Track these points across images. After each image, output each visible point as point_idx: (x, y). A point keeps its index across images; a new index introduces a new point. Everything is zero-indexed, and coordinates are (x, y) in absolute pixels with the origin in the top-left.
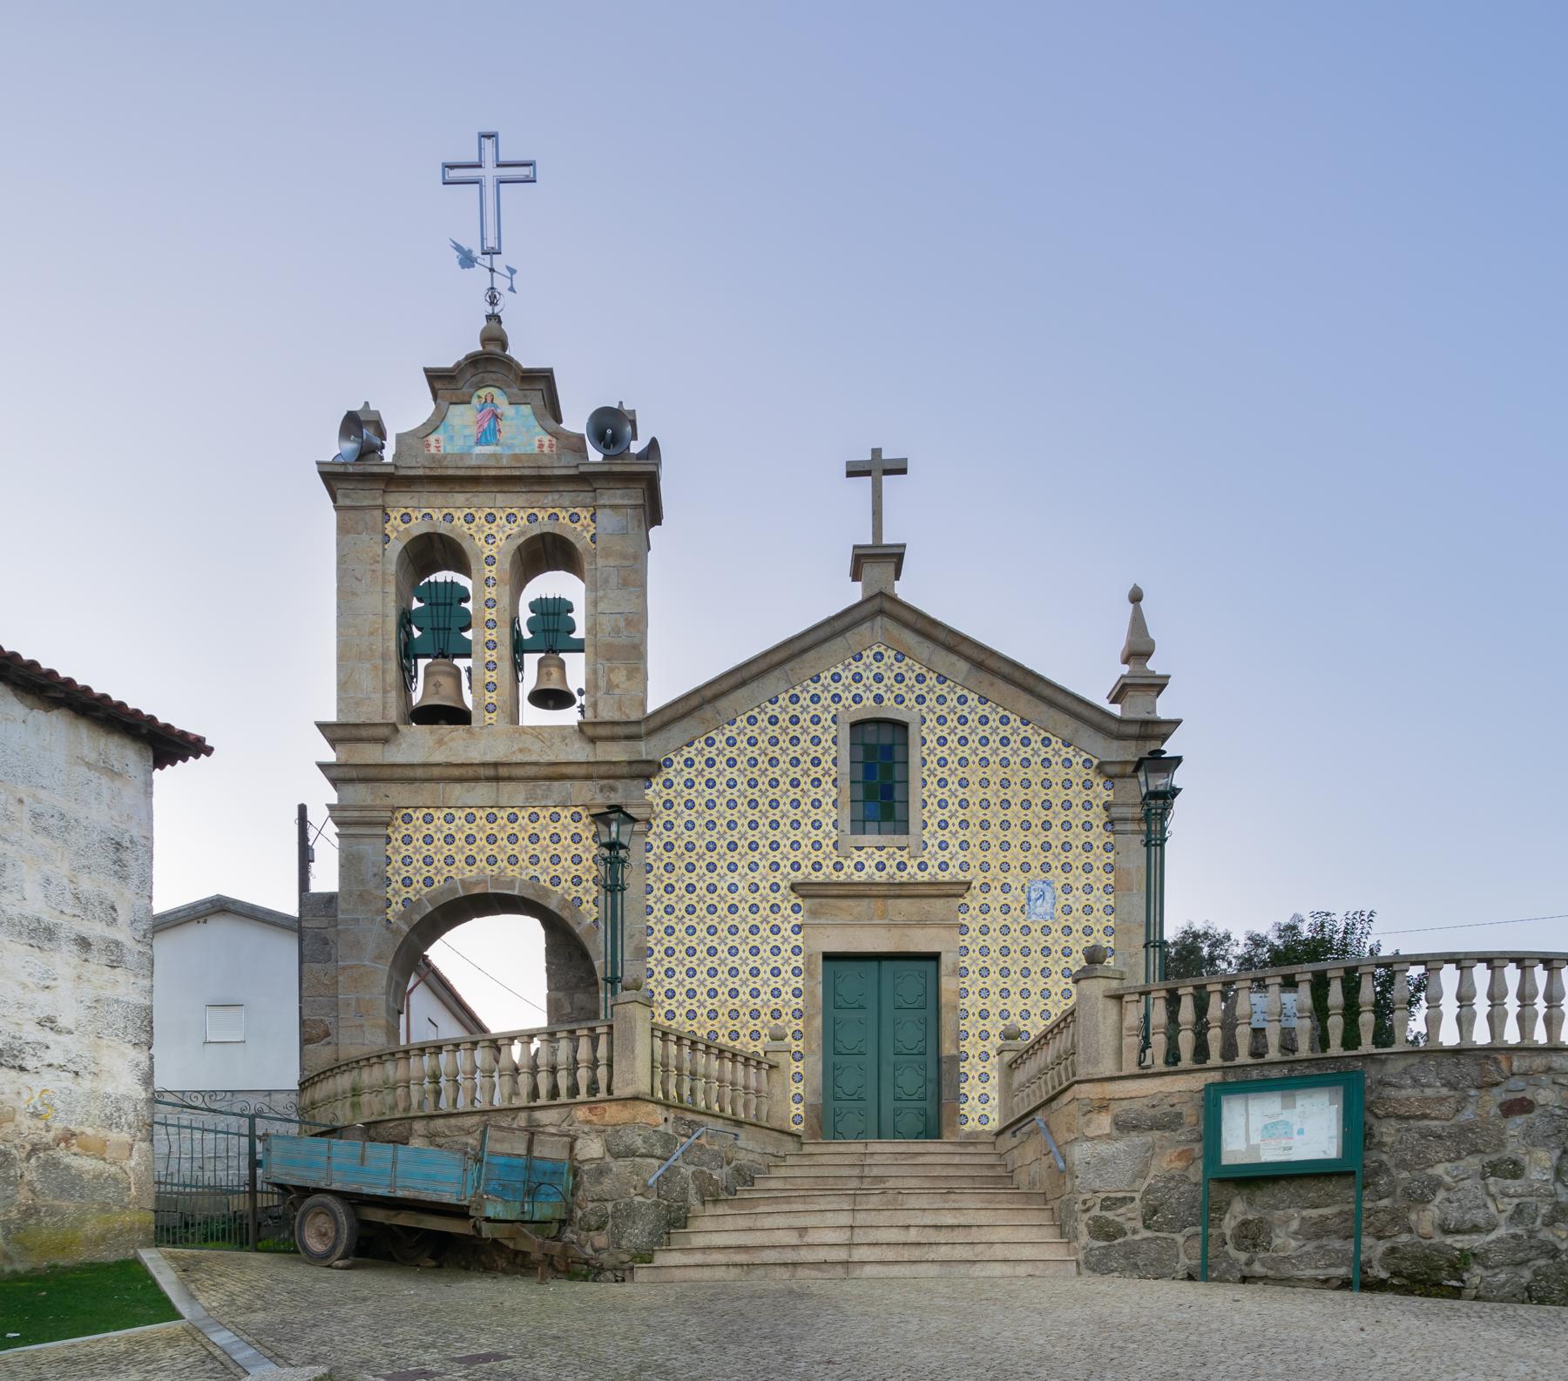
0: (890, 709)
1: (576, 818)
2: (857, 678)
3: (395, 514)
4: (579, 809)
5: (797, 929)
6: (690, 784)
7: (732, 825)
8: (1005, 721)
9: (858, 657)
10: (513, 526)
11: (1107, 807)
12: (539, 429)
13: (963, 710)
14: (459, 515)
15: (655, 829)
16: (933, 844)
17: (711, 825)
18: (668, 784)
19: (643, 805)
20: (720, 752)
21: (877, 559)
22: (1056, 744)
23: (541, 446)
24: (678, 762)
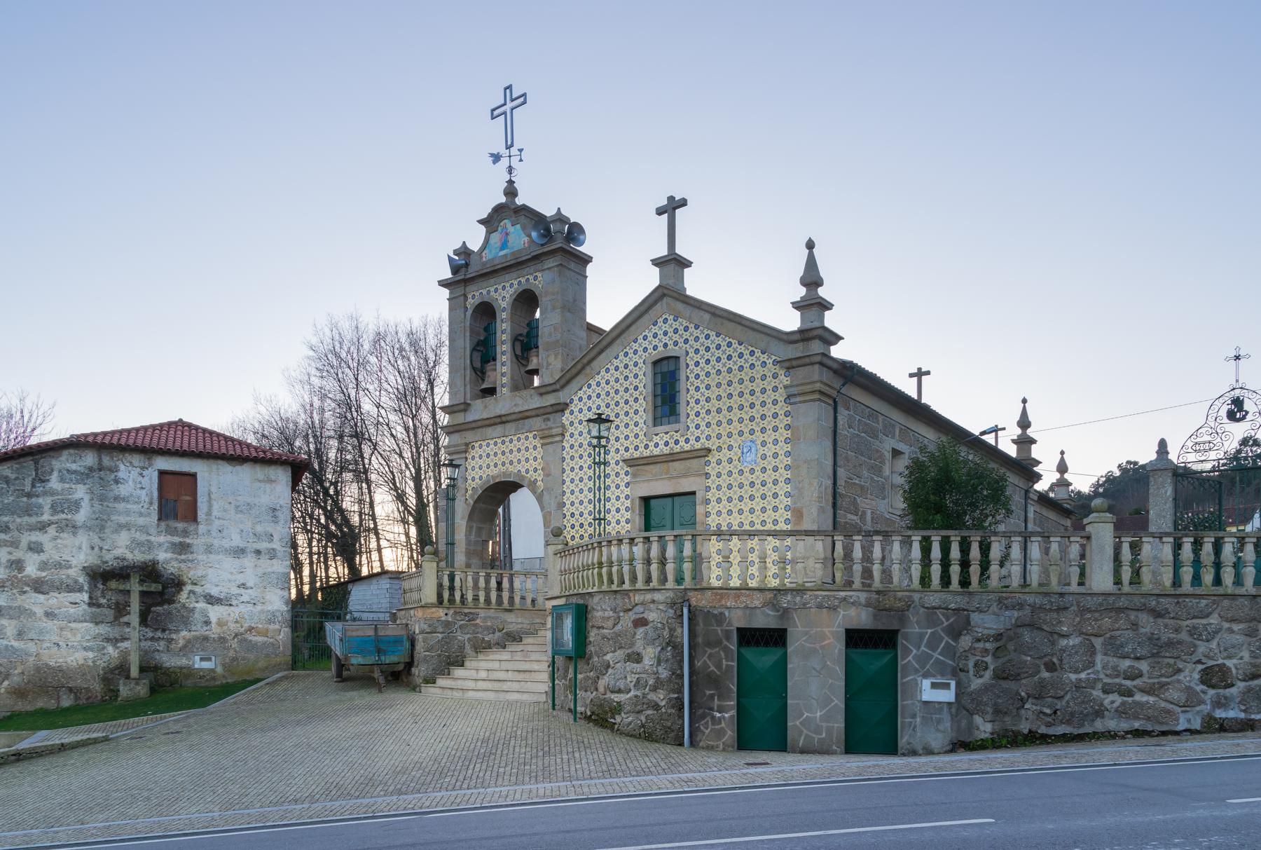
0: (672, 351)
2: (655, 336)
5: (627, 485)
8: (729, 345)
9: (655, 324)
11: (786, 387)
13: (708, 343)
16: (692, 426)
21: (673, 264)
22: (758, 353)
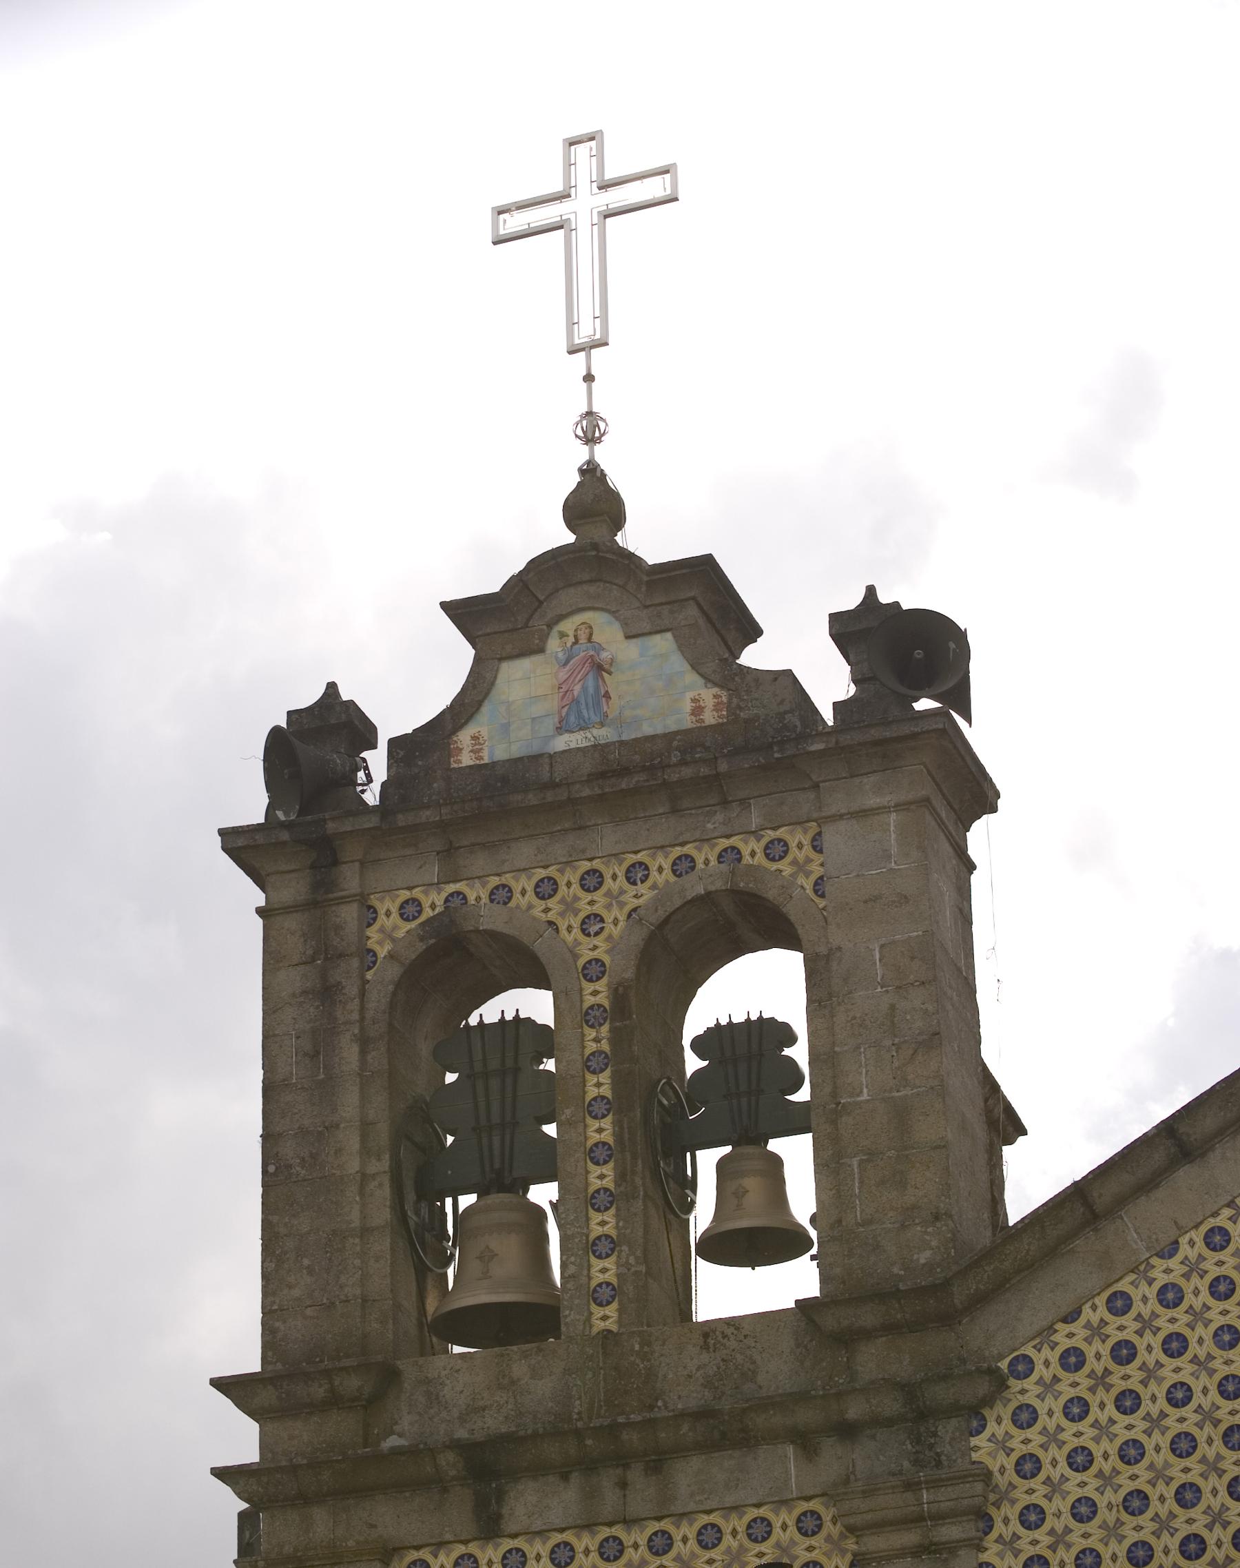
1: (808, 1525)
3: (387, 906)
4: (814, 1505)
6: (1077, 1410)
7: (1187, 1495)
10: (642, 888)
12: (692, 678)
14: (523, 885)
15: (999, 1528)
17: (1136, 1502)
18: (1025, 1417)
19: (963, 1478)
20: (1146, 1324)
23: (697, 710)
24: (1046, 1360)
